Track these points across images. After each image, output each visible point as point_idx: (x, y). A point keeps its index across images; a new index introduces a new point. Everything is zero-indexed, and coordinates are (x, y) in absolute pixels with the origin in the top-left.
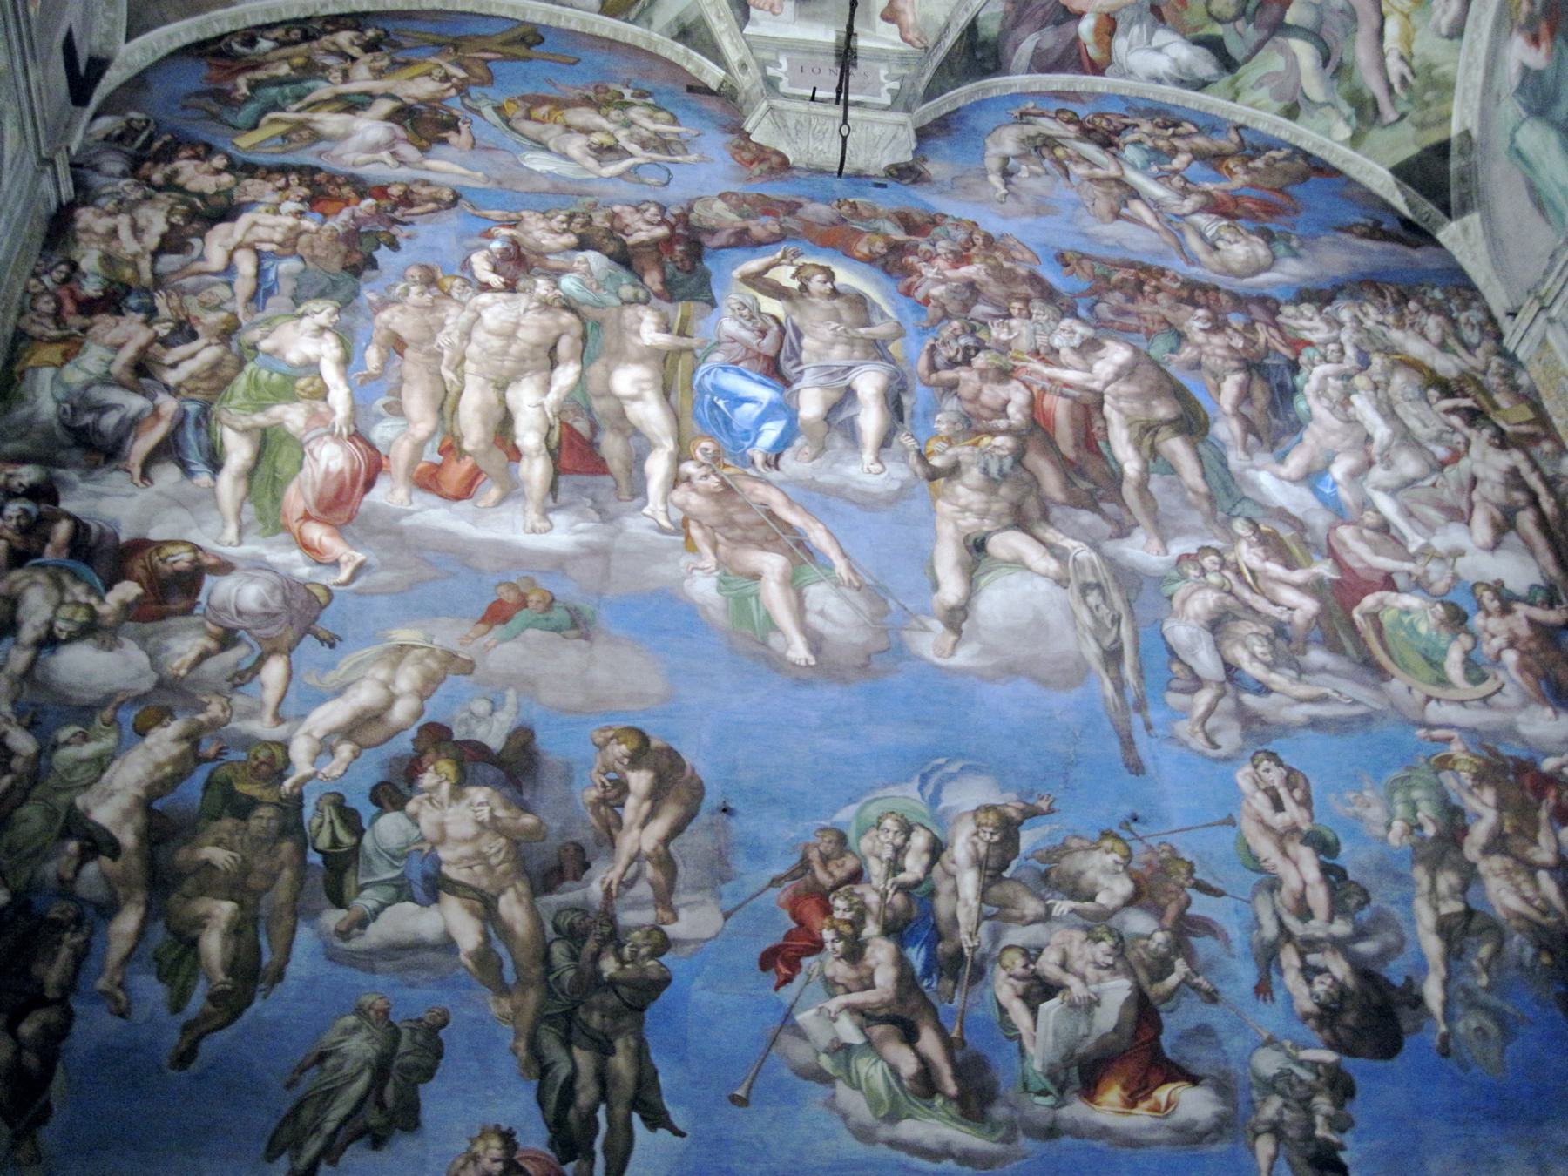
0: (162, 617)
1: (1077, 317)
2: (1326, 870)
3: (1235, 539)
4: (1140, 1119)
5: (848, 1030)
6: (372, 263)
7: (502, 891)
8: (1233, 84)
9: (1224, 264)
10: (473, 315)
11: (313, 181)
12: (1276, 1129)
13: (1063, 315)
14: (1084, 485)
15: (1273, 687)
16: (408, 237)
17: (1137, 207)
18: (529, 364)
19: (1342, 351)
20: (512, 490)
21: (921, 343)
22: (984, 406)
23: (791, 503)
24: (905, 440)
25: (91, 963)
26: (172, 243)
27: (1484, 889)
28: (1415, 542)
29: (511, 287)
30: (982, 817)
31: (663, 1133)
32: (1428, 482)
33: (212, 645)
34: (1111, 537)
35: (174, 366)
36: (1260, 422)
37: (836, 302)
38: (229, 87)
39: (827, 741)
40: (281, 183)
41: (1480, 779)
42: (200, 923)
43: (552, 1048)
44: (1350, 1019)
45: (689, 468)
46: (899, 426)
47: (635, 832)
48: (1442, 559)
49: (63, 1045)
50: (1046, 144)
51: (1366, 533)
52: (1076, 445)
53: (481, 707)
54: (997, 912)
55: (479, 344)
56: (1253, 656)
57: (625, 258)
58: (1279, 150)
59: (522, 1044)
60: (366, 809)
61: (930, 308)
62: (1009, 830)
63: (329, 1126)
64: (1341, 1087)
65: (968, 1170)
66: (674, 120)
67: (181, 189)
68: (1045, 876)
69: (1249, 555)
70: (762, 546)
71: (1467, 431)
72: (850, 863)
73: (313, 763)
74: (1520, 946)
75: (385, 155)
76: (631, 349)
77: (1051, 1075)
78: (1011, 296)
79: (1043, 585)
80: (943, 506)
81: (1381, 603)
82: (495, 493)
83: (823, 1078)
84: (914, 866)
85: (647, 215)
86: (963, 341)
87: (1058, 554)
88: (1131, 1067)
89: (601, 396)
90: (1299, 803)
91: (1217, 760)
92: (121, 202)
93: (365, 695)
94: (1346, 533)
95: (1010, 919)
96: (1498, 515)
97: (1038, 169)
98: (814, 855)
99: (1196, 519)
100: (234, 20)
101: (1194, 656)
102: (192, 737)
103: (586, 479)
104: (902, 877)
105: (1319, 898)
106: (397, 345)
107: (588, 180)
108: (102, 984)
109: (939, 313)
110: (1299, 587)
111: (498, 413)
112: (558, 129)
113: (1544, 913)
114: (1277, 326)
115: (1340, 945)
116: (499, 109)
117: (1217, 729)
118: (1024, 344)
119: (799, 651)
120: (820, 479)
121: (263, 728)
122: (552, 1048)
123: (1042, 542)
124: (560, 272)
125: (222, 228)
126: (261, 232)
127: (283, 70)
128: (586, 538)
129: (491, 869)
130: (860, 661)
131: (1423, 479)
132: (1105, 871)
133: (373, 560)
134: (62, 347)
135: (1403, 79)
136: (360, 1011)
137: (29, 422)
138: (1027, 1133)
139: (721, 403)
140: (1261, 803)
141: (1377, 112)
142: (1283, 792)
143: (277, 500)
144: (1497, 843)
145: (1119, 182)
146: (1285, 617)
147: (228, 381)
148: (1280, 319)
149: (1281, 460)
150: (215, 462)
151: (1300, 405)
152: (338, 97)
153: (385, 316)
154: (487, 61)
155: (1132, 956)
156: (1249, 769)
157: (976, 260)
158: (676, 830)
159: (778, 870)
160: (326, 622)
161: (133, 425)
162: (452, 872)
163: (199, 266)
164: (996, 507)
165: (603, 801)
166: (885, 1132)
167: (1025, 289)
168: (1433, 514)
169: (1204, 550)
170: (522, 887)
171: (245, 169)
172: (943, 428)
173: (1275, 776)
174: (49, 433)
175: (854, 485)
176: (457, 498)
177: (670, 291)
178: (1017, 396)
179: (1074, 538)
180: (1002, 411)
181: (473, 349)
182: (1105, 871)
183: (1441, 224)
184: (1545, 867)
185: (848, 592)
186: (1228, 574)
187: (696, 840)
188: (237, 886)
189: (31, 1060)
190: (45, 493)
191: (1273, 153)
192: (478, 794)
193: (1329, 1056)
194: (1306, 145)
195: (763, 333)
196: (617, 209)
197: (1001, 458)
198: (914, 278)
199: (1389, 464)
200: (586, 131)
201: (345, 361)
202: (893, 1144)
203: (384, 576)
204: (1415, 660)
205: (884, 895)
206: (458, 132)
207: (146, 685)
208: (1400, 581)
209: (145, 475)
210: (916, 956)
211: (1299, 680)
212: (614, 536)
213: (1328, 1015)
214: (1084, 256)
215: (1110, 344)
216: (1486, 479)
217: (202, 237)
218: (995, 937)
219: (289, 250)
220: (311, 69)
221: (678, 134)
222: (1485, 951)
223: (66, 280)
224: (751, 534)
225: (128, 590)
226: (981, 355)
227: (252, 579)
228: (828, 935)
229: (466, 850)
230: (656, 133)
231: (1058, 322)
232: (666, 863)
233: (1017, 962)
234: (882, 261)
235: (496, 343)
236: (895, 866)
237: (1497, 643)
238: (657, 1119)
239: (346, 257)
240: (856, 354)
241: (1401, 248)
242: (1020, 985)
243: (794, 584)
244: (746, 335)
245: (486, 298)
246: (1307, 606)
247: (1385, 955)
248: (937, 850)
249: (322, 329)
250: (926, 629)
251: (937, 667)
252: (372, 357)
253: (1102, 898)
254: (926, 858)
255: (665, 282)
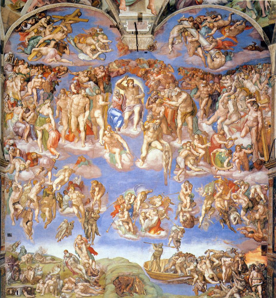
0: (34, 166)
1: (178, 87)
2: (191, 201)
3: (194, 139)
4: (155, 235)
5: (121, 223)
6: (55, 89)
7: (80, 205)
8: (231, 4)
9: (213, 66)
10: (72, 101)
11: (43, 68)
12: (173, 237)
13: (175, 87)
14: (170, 130)
15: (192, 169)
16: (60, 82)
17: (200, 50)
18: (81, 112)
19: (231, 89)
20: (80, 139)
21: (147, 98)
22: (156, 113)
23: (122, 138)
24: (141, 123)
25: (33, 216)
26: (22, 89)
27: (215, 204)
28: (229, 136)
29: (78, 93)
30: (142, 193)
31: (98, 236)
32: (236, 122)
33: (41, 170)
34: (172, 141)
35: (27, 118)
36: (207, 111)
37: (134, 89)
38: (24, 41)
39: (122, 182)
40: (37, 70)
41: (222, 185)
42: (45, 211)
43: (86, 226)
44: (187, 223)
45: (106, 132)
46: (141, 119)
47: (96, 197)
48: (232, 140)
49: (33, 226)
50: (185, 30)
51: (220, 136)
52: (171, 120)
53: (76, 178)
54: (141, 207)
55: (74, 108)
56: (190, 163)
57: (96, 83)
58: (239, 21)
59: (82, 225)
60: (63, 195)
61: (150, 89)
62: (146, 195)
63: (62, 235)
64: (183, 231)
65: (133, 241)
66: (107, 39)
67: (21, 73)
68: (149, 202)
69: (196, 143)
70: (116, 147)
71: (250, 108)
72: (123, 201)
73: (56, 188)
74: (217, 213)
75: (54, 59)
76: (98, 107)
77: (145, 229)
78: (166, 83)
79: (159, 151)
80: (145, 137)
81: (217, 151)
82: (77, 140)
83: (117, 229)
84: (132, 201)
85: (101, 70)
86: (155, 97)
87: (162, 144)
88: (156, 228)
89: (93, 118)
90: (190, 190)
91: (179, 182)
92: (12, 79)
93: (61, 177)
94: (216, 136)
95: (143, 208)
96: (248, 129)
97: (180, 41)
98: (119, 199)
99: (188, 136)
100: (22, 20)
101: (180, 164)
102: (41, 185)
103: (90, 136)
104: (130, 202)
105: (188, 205)
106: (61, 109)
107: (91, 61)
108: (35, 219)
109: (152, 89)
110: (202, 148)
111: (77, 123)
112: (85, 45)
113: (223, 207)
114: (219, 83)
115: (189, 212)
116: (73, 40)
117: (181, 177)
118: (166, 96)
119: (120, 167)
120: (127, 133)
121: (49, 183)
122: (86, 226)
123: (160, 143)
124: (86, 88)
125: (30, 83)
126: (36, 84)
127: (33, 34)
128: (90, 148)
129: (78, 202)
130: (128, 168)
131: (236, 121)
132: (158, 201)
133: (61, 154)
134: (11, 115)
135: (268, 6)
136: (64, 221)
137: (9, 131)
138: (141, 236)
139: (112, 117)
140: (184, 190)
141: (262, 14)
142: (188, 188)
143: (46, 144)
144: (221, 196)
145: (197, 41)
146: (198, 155)
147: (36, 120)
148: (221, 81)
149: (208, 120)
150: (37, 138)
151: (217, 105)
152: (44, 41)
153: (58, 103)
154: (71, 24)
155: (159, 214)
156: (184, 184)
157: (162, 73)
158: (101, 196)
159: (114, 202)
160: (56, 166)
161: (24, 130)
162: (74, 203)
163: (27, 93)
164: (154, 136)
165: (92, 192)
166: (124, 236)
167: (170, 80)
168: (234, 130)
169: (188, 142)
170: (82, 205)
171: (30, 66)
172: (148, 119)
173: (187, 186)
174: (13, 133)
175: (132, 133)
176: (71, 141)
177: (105, 90)
178: (162, 109)
179: (166, 141)
180: (159, 114)
181: (72, 109)
182: (158, 201)
183: (269, 44)
184: (226, 200)
185: (128, 155)
186: (191, 147)
187: (104, 198)
188: (48, 206)
189: (29, 228)
190: (14, 145)
191: (238, 23)
192: (77, 192)
193: (183, 228)
194: (246, 18)
195: (120, 99)
196: (96, 68)
197: (157, 125)
198: (148, 80)
199: (230, 118)
200: (90, 45)
201: (53, 114)
202: (124, 237)
203: (62, 157)
204: (219, 163)
205: (127, 205)
206: (67, 49)
207: (34, 177)
208: (222, 146)
209: (27, 140)
210: (130, 213)
211: (197, 167)
212: (94, 147)
213: (184, 222)
214: (184, 68)
215: (183, 93)
216: (250, 120)
217: (27, 86)
218: (141, 211)
219: (41, 88)
220: (38, 32)
221: (108, 43)
222: (211, 213)
223: (8, 99)
224: (115, 145)
225: (29, 162)
226: (158, 100)
227: (45, 159)
228: (120, 211)
229: (75, 200)
230: (103, 43)
231: (174, 89)
232: (100, 201)
233: (143, 214)
234: (143, 76)
235: (76, 107)
236: (129, 201)
237: (236, 158)
238: (97, 234)
239: (50, 88)
240: (136, 102)
241: (257, 52)
242: (143, 217)
243: (120, 155)
244: (117, 100)
245: (74, 96)
246: (203, 152)
247: (195, 214)
248: (135, 198)
249: (49, 107)
250: (139, 161)
251: (139, 168)
252: (57, 112)
253: (157, 205)
254: (134, 200)
255: (104, 88)
